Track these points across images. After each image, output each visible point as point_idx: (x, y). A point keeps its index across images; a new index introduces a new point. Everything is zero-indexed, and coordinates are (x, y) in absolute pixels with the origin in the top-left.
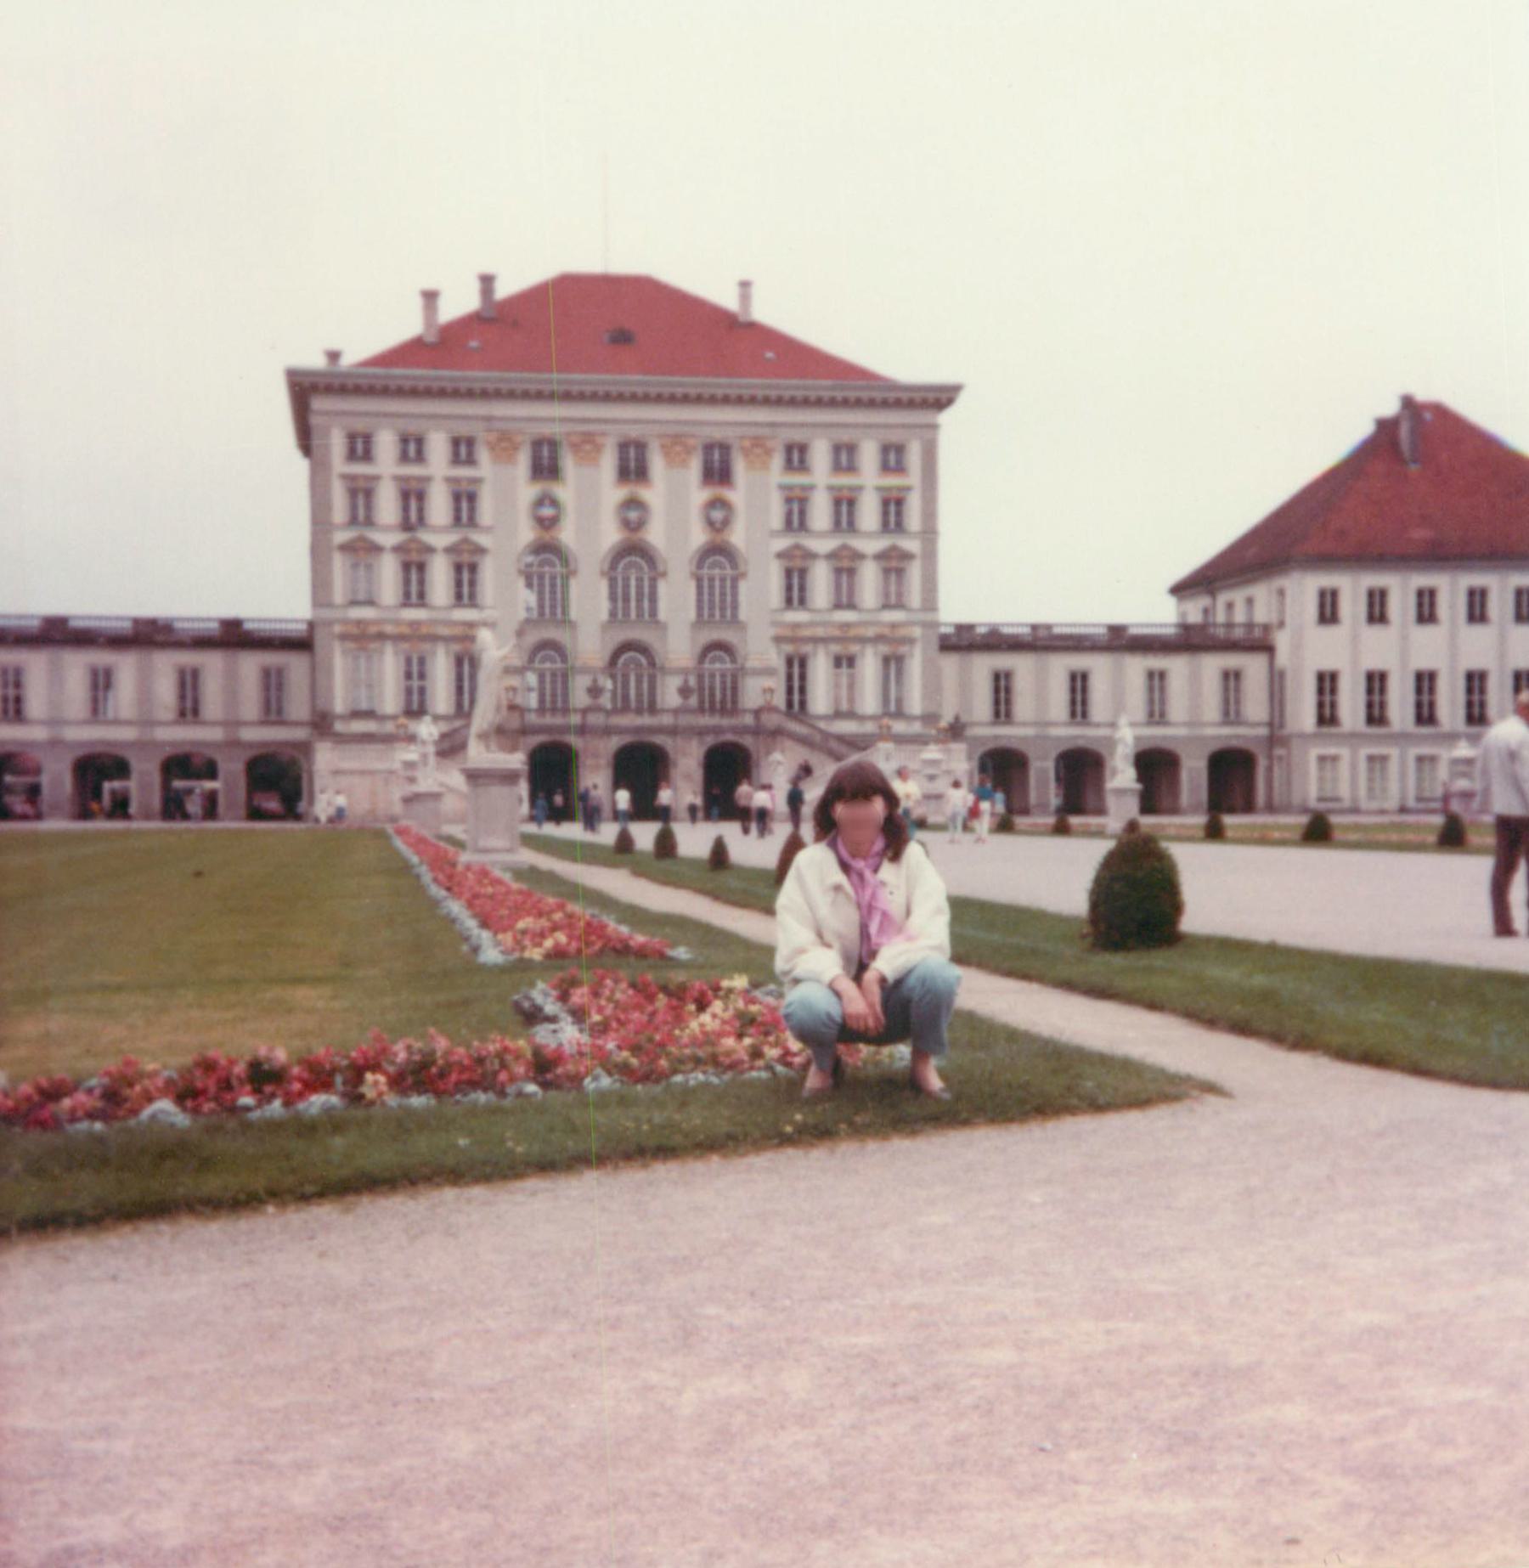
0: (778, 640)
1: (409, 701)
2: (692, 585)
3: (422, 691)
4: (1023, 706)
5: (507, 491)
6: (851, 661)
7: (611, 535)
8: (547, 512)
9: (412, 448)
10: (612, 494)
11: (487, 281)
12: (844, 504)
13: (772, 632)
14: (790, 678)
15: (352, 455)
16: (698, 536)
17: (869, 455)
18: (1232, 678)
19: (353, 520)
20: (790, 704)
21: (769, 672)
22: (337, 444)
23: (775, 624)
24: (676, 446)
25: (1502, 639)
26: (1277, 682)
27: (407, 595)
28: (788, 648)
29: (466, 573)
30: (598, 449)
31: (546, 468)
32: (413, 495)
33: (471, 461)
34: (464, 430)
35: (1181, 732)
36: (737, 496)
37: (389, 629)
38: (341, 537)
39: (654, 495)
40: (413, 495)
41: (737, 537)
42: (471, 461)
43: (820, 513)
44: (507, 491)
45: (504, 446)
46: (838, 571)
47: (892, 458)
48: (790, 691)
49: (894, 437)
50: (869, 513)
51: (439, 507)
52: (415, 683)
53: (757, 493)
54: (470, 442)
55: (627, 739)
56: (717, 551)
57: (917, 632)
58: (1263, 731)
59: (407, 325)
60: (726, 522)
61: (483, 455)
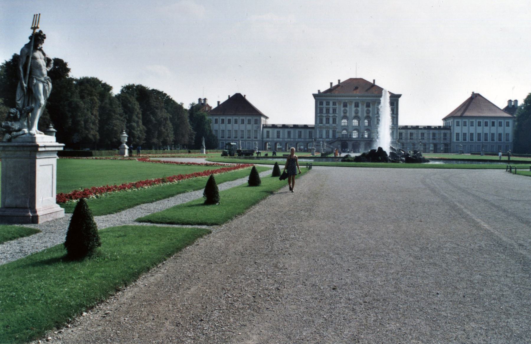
5: (340, 109)
9: (328, 104)
10: (354, 109)
11: (339, 81)
15: (320, 105)
16: (365, 115)
19: (320, 113)
22: (318, 104)
24: (363, 102)
25: (483, 129)
32: (328, 110)
33: (335, 105)
34: (335, 101)
36: (370, 109)
38: (319, 115)
39: (359, 109)
41: (371, 115)
42: (335, 105)
51: (331, 111)
59: (328, 87)
61: (337, 104)
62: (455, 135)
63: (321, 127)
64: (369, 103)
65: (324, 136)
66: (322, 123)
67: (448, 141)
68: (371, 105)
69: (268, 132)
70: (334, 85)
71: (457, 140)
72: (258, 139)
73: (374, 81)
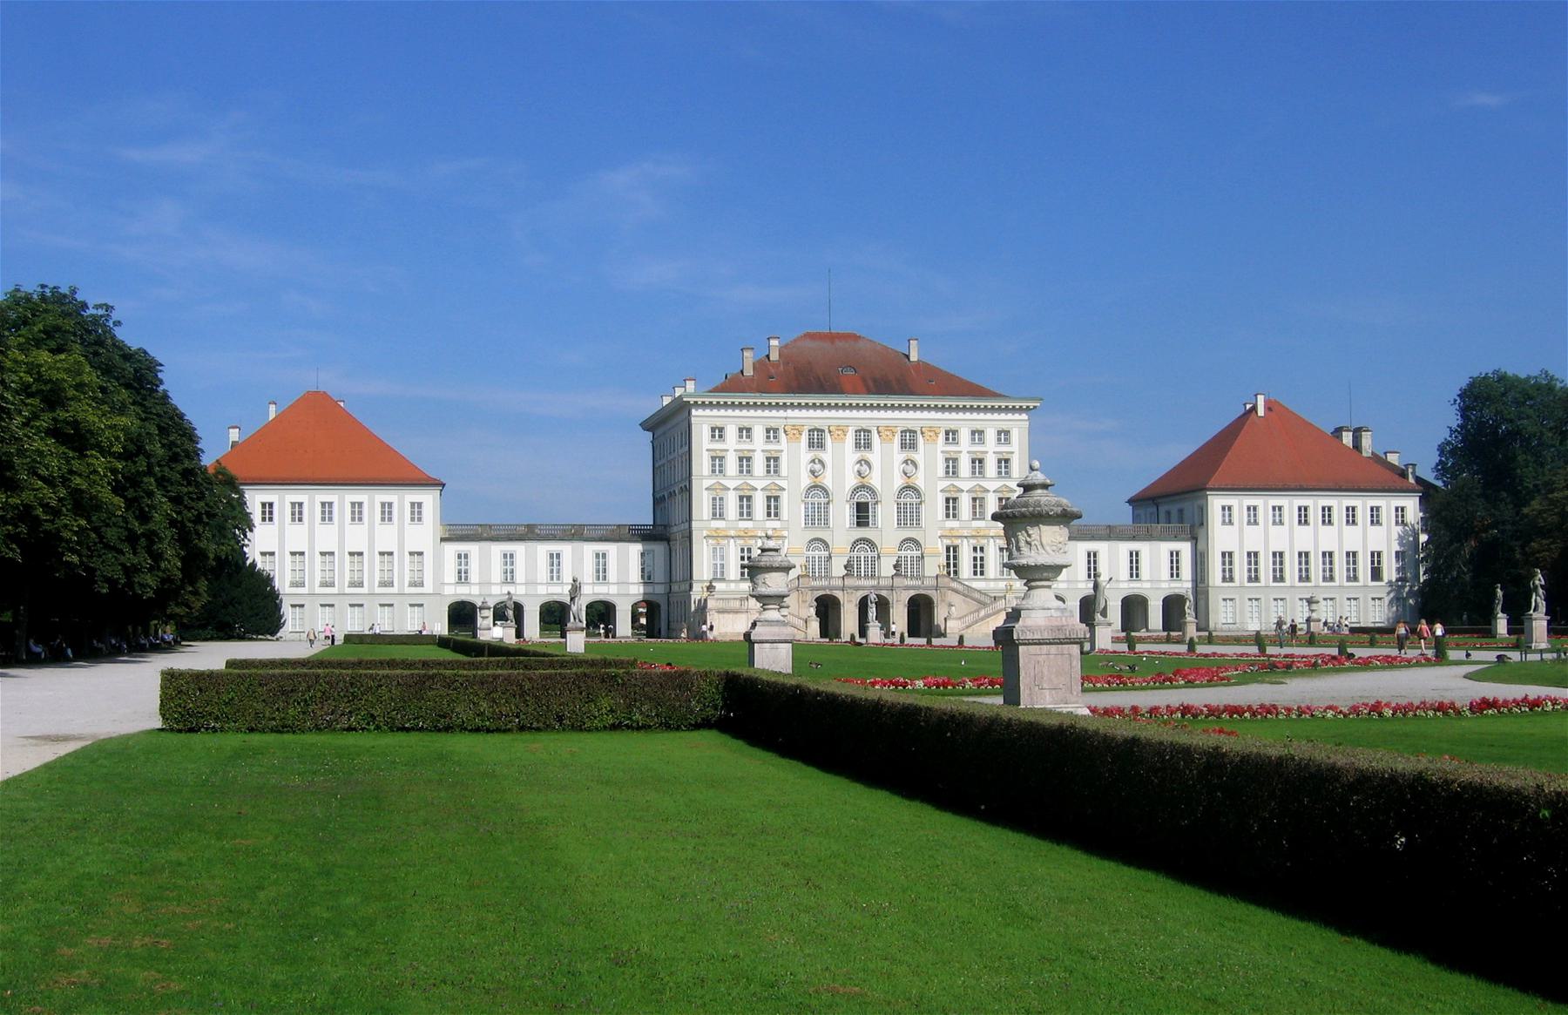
5: (796, 457)
6: (982, 549)
7: (851, 481)
9: (745, 432)
10: (851, 455)
12: (978, 463)
16: (899, 482)
17: (991, 435)
18: (1175, 557)
21: (937, 555)
22: (706, 432)
26: (1200, 561)
27: (741, 514)
35: (1147, 585)
36: (918, 457)
37: (732, 533)
38: (707, 483)
39: (874, 456)
41: (919, 481)
43: (965, 467)
47: (1003, 436)
51: (759, 465)
53: (931, 454)
54: (776, 430)
56: (909, 488)
58: (1189, 585)
61: (782, 435)
62: (1219, 559)
63: (715, 536)
66: (721, 516)
67: (1184, 585)
69: (462, 557)
71: (1224, 579)
72: (428, 587)
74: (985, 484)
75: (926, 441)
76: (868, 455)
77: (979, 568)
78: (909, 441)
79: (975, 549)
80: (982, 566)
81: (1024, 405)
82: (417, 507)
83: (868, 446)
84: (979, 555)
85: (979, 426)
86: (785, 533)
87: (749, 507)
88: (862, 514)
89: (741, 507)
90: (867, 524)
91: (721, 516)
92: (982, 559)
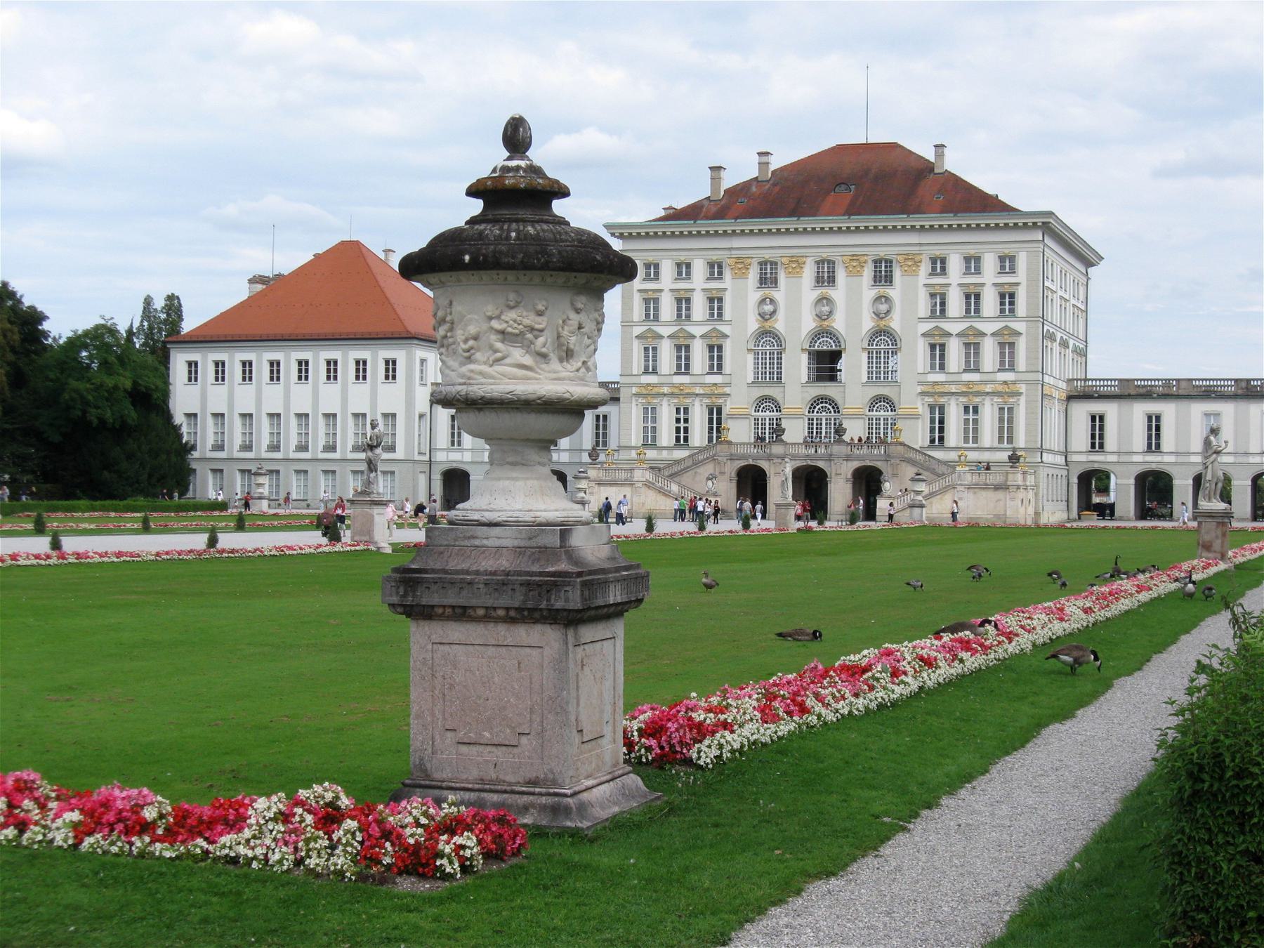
0: (922, 393)
1: (678, 439)
2: (865, 356)
3: (686, 430)
4: (1168, 442)
6: (976, 410)
7: (809, 324)
8: (768, 308)
9: (684, 269)
10: (809, 294)
12: (973, 299)
13: (919, 389)
14: (932, 421)
16: (868, 324)
17: (990, 263)
20: (932, 441)
21: (915, 417)
23: (920, 383)
24: (855, 263)
27: (679, 367)
28: (931, 400)
29: (715, 352)
30: (801, 266)
31: (768, 279)
32: (683, 302)
34: (715, 256)
36: (894, 293)
37: (666, 390)
38: (638, 330)
39: (838, 294)
40: (683, 302)
41: (895, 323)
43: (955, 304)
44: (743, 295)
45: (741, 266)
46: (967, 345)
47: (1007, 263)
48: (932, 430)
49: (1007, 249)
50: (990, 303)
51: (699, 308)
52: (682, 425)
54: (720, 266)
55: (799, 464)
57: (1023, 388)
59: (698, 191)
60: (888, 312)
61: (727, 274)
64: (889, 263)
65: (666, 436)
66: (655, 372)
68: (897, 273)
70: (730, 180)
73: (939, 147)
74: (981, 326)
75: (905, 273)
76: (832, 293)
77: (972, 431)
78: (883, 274)
79: (966, 409)
80: (976, 430)
81: (1030, 221)
82: (391, 365)
83: (832, 280)
84: (971, 417)
85: (972, 250)
86: (727, 390)
87: (687, 358)
88: (826, 364)
89: (679, 358)
90: (833, 378)
91: (655, 372)
92: (976, 421)
